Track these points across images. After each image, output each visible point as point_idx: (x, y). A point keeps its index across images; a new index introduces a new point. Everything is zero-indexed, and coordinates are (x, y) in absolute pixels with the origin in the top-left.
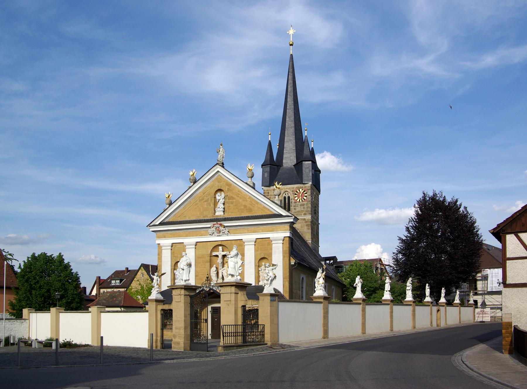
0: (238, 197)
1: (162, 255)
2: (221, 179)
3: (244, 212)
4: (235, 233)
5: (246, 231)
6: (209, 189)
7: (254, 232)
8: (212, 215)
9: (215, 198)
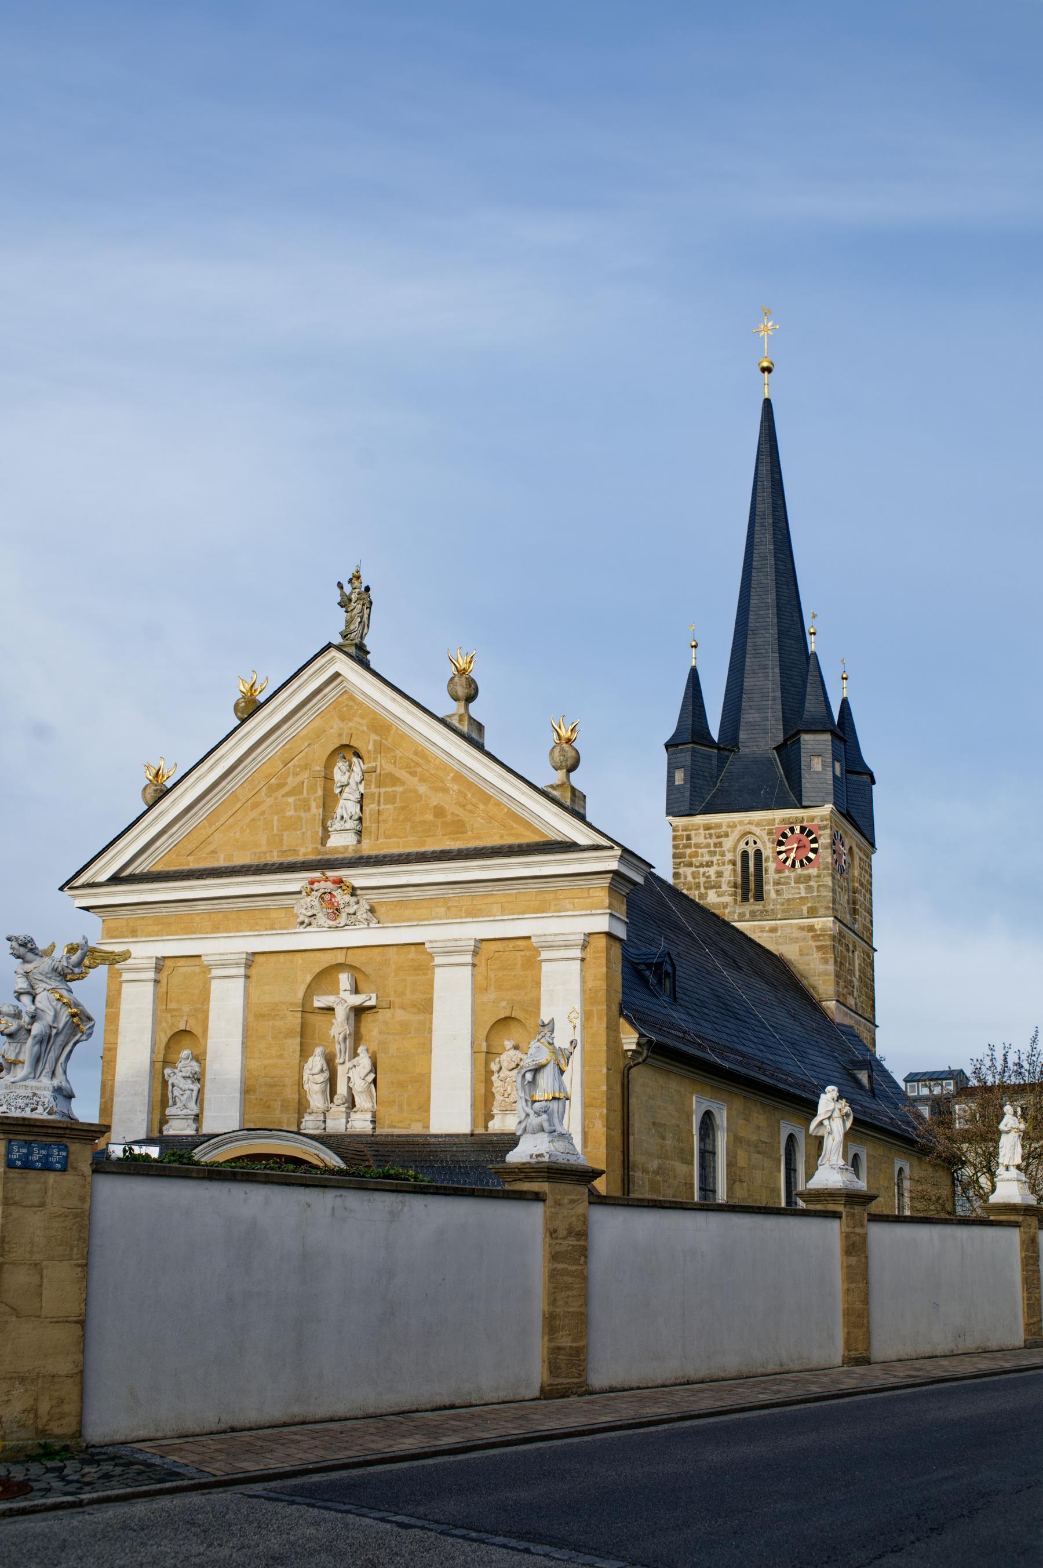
0: (413, 774)
1: (120, 1005)
2: (352, 706)
3: (433, 836)
4: (398, 921)
5: (438, 909)
6: (306, 744)
7: (474, 913)
8: (315, 846)
9: (328, 778)
